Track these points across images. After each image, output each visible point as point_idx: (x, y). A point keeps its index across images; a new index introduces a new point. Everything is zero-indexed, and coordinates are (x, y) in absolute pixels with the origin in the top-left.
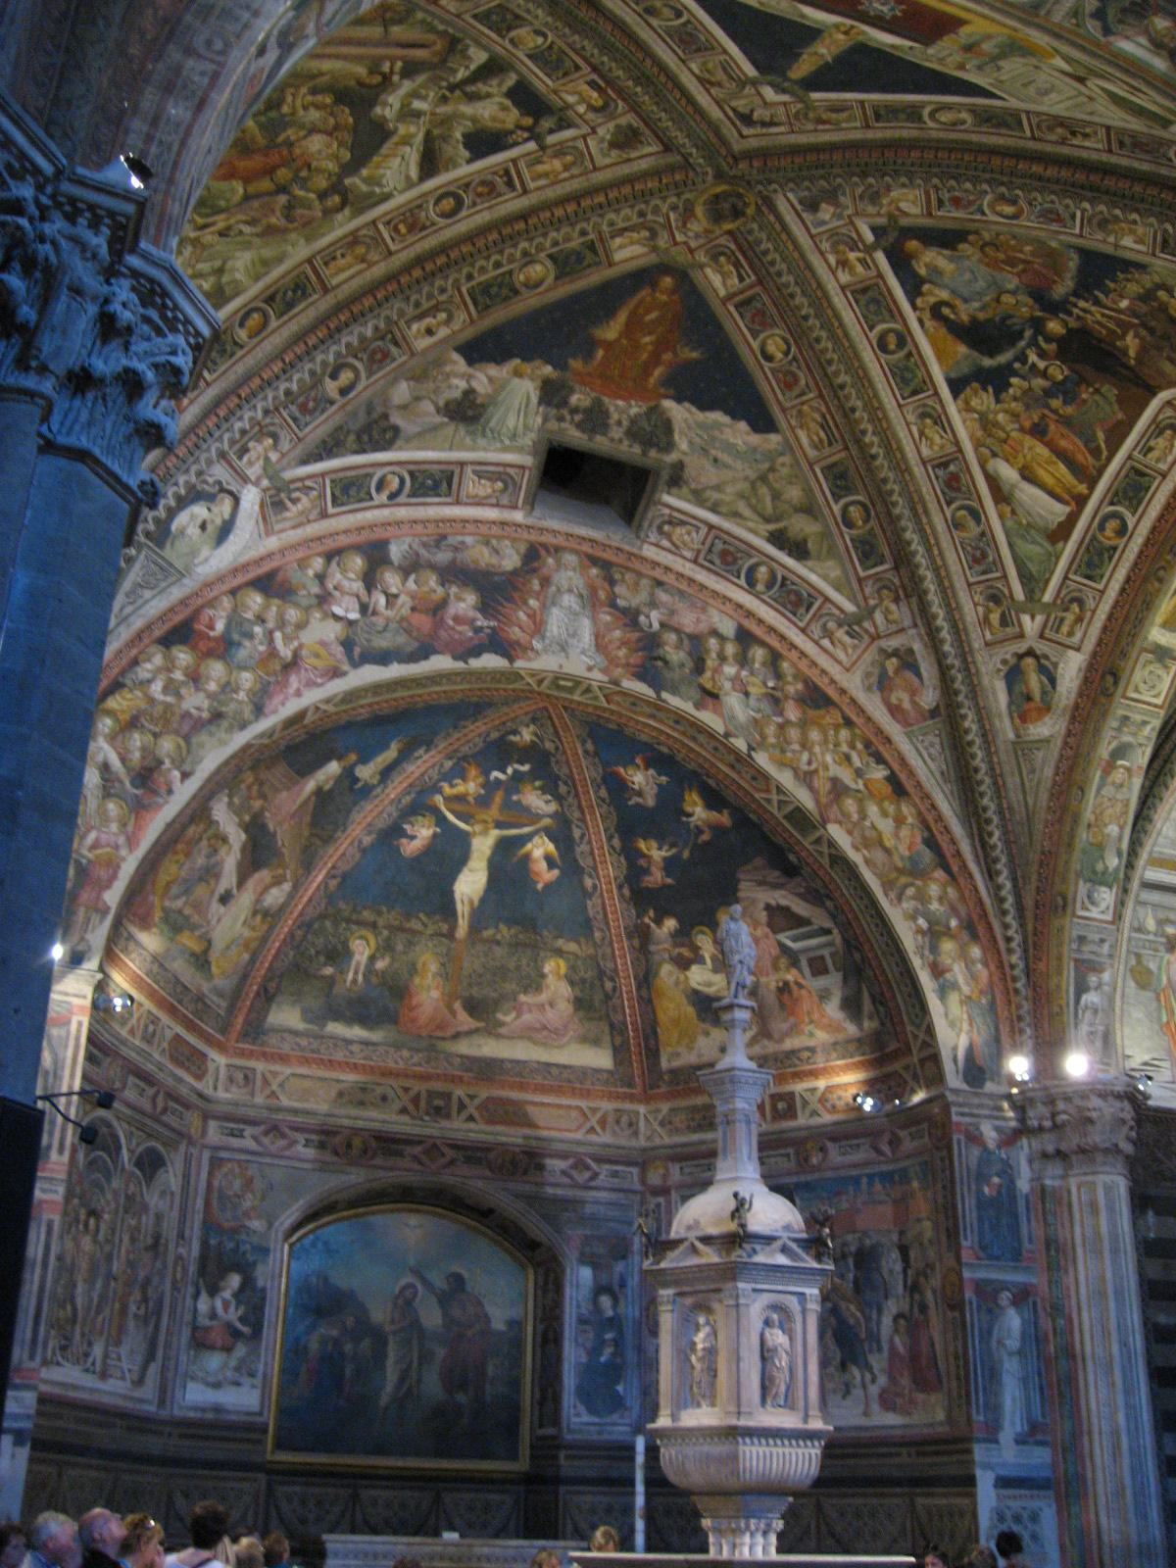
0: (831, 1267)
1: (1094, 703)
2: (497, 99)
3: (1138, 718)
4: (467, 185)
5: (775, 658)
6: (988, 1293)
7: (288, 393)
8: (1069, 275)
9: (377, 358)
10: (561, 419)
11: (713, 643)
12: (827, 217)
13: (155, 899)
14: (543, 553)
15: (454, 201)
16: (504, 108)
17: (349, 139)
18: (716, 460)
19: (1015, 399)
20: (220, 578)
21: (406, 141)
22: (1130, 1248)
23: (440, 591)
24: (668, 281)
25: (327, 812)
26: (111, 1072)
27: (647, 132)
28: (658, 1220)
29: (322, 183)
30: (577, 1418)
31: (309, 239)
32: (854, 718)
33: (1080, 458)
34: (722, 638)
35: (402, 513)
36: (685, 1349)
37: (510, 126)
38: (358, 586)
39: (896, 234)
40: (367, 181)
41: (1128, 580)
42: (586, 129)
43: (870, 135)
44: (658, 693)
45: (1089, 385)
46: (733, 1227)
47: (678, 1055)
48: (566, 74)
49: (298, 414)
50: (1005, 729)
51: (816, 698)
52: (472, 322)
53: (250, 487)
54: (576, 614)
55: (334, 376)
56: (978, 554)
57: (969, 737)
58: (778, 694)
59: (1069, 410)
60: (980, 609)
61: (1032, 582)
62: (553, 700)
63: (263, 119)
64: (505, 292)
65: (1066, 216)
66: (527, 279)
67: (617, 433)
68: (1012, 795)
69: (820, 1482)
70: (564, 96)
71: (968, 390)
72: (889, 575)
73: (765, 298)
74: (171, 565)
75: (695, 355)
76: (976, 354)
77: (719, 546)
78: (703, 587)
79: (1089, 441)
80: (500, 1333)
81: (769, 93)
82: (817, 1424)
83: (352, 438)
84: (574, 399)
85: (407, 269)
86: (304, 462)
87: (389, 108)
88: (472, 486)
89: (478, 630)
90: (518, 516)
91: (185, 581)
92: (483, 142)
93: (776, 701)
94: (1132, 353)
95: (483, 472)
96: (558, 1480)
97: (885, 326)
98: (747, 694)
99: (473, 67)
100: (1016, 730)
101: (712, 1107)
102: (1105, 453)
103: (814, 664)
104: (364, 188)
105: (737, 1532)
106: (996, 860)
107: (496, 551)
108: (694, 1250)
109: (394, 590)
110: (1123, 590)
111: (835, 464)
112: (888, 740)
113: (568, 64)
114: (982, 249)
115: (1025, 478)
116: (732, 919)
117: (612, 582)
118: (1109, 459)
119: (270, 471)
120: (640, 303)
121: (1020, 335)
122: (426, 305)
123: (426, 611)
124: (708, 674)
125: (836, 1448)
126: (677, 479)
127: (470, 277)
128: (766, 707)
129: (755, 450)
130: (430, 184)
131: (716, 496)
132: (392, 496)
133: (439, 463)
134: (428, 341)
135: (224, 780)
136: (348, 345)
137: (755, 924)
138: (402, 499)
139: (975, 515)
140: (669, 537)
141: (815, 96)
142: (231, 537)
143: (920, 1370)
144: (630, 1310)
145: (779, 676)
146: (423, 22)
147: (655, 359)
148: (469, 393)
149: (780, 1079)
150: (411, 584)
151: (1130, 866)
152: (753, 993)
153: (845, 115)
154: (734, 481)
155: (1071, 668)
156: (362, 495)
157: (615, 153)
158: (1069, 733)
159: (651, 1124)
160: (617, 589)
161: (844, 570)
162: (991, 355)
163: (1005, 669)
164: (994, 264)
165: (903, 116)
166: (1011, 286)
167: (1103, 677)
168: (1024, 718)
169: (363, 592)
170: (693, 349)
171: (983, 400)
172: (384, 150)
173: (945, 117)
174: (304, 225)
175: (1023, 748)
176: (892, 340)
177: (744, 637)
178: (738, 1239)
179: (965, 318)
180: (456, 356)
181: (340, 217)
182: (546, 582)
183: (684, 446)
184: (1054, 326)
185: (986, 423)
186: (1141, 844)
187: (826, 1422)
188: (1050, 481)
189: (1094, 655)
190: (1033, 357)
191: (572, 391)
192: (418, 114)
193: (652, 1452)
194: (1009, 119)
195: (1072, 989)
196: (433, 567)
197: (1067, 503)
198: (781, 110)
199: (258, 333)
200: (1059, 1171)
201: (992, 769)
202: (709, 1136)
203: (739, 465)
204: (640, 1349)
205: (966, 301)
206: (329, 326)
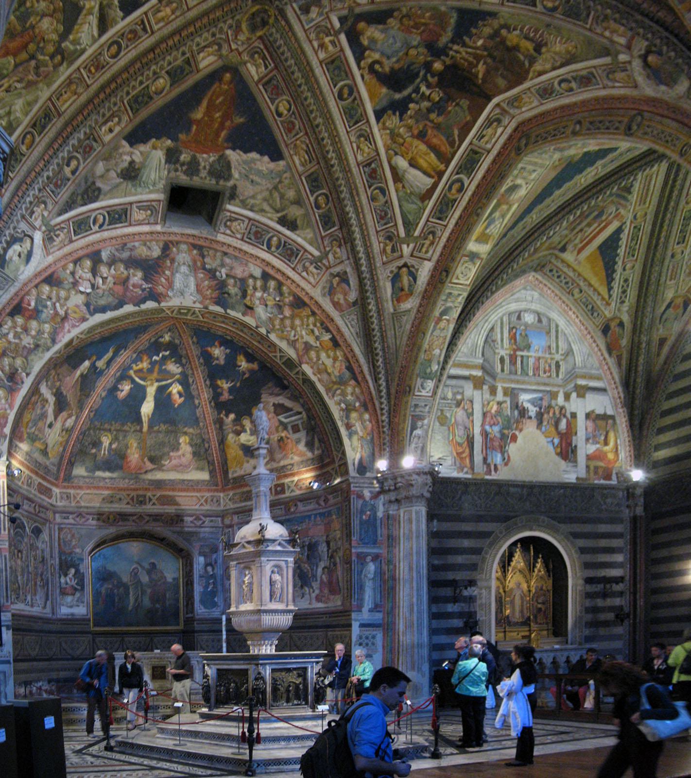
0: (298, 550)
3: (456, 293)
4: (123, 35)
6: (362, 557)
7: (48, 178)
13: (23, 429)
22: (424, 535)
25: (86, 383)
26: (17, 499)
28: (229, 537)
30: (200, 610)
31: (49, 85)
36: (240, 584)
46: (259, 537)
47: (236, 472)
54: (187, 276)
62: (179, 320)
68: (390, 340)
69: (291, 628)
76: (392, 92)
80: (170, 583)
82: (291, 607)
85: (97, 95)
94: (480, 76)
96: (194, 632)
101: (250, 491)
102: (457, 143)
105: (260, 645)
106: (379, 373)
108: (244, 547)
116: (259, 410)
120: (214, 92)
122: (108, 115)
125: (297, 616)
127: (128, 93)
129: (272, 172)
133: (120, 205)
135: (44, 375)
136: (73, 145)
137: (268, 413)
143: (333, 587)
144: (219, 571)
149: (279, 478)
150: (113, 271)
151: (443, 368)
152: (267, 443)
159: (226, 500)
164: (407, 30)
166: (415, 43)
178: (261, 541)
179: (387, 69)
184: (438, 66)
186: (450, 357)
187: (295, 605)
189: (438, 261)
190: (423, 88)
193: (229, 620)
195: (409, 429)
200: (396, 508)
201: (381, 328)
202: (249, 503)
204: (223, 585)
205: (388, 58)
206: (63, 136)
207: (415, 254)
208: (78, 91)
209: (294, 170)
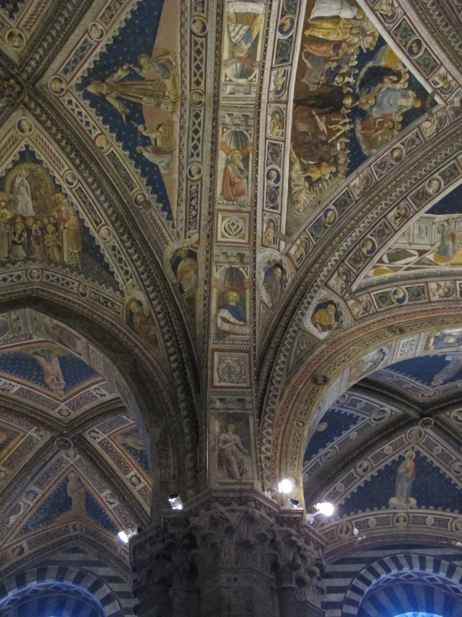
8: (361, 139)
19: (352, 54)
33: (314, 47)
45: (323, 84)
71: (375, 44)
97: (420, 54)
114: (394, 123)
115: (338, 17)
118: (300, 57)
121: (361, 86)
162: (370, 69)
165: (448, 174)
171: (367, 43)
176: (415, 49)
185: (363, 33)
188: (326, 25)
194: (419, 202)
197: (313, 19)
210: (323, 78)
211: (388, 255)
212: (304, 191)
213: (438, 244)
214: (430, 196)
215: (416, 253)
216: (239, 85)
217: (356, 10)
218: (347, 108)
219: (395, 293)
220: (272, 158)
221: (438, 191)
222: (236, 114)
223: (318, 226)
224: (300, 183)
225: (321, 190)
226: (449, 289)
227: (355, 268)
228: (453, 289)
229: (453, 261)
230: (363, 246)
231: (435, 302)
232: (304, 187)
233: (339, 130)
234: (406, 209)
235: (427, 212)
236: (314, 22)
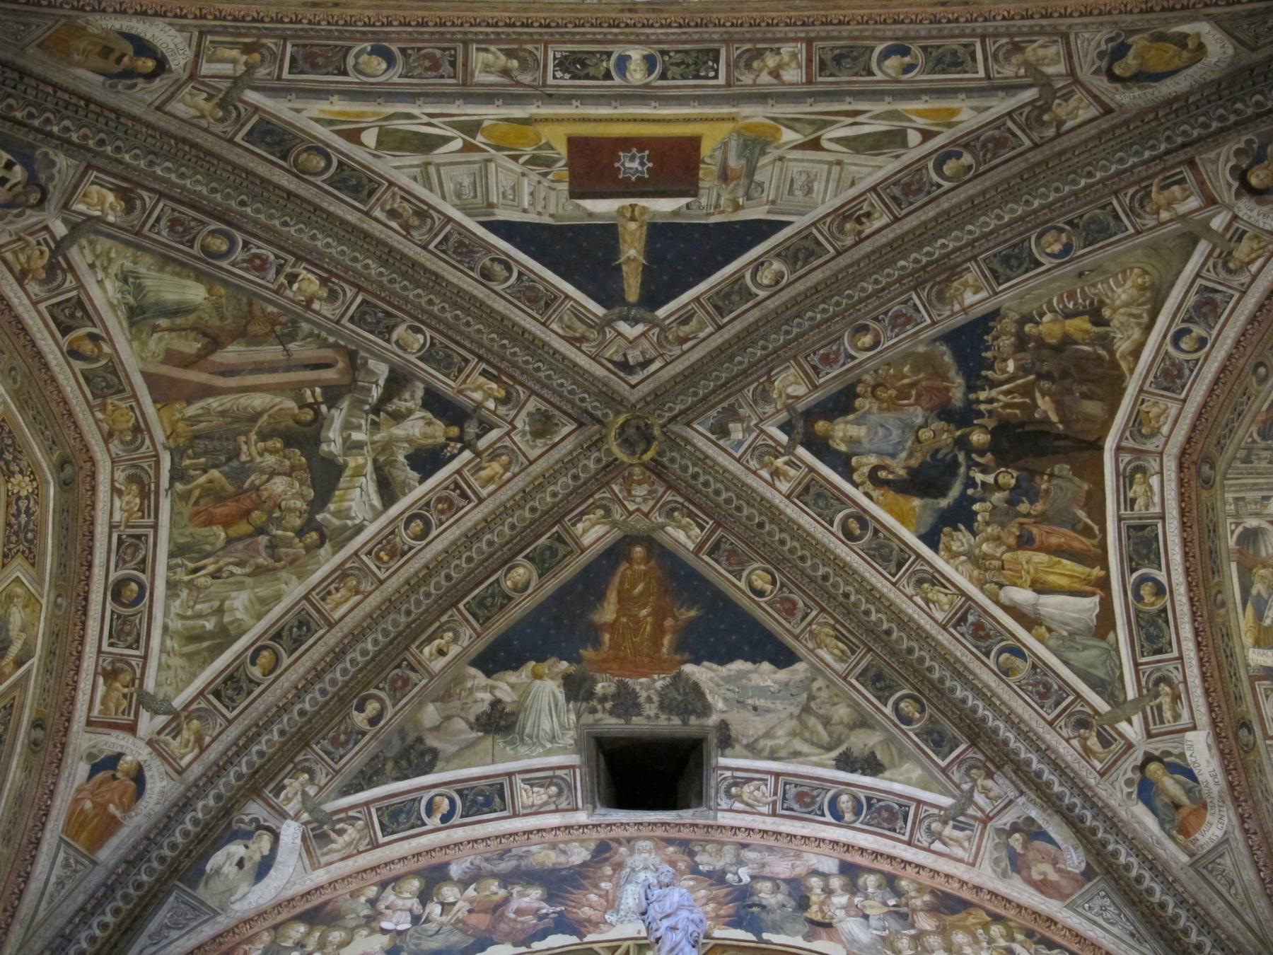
1: (1246, 769)
2: (419, 414)
5: (890, 882)
8: (952, 373)
9: (400, 687)
10: (593, 711)
11: (815, 882)
12: (740, 436)
14: (614, 845)
15: (421, 520)
16: (429, 424)
17: (306, 476)
18: (755, 709)
19: (988, 524)
20: (262, 914)
21: (359, 472)
23: (502, 893)
24: (638, 551)
27: (557, 413)
29: (298, 522)
31: (301, 577)
32: (1003, 912)
33: (1076, 545)
34: (825, 876)
35: (459, 834)
37: (442, 440)
38: (414, 903)
39: (801, 423)
40: (338, 514)
41: (1197, 632)
42: (507, 427)
43: (727, 334)
44: (758, 934)
45: (1042, 474)
48: (460, 371)
49: (330, 748)
50: (1172, 853)
51: (948, 905)
52: (479, 636)
53: (288, 821)
55: (360, 709)
56: (1041, 688)
57: (1134, 873)
58: (905, 910)
59: (1039, 507)
60: (1075, 742)
61: (1108, 687)
63: (226, 468)
64: (499, 601)
65: (911, 312)
66: (515, 584)
67: (651, 710)
70: (469, 393)
71: (943, 539)
72: (970, 754)
73: (731, 538)
74: (203, 903)
75: (693, 613)
77: (792, 791)
78: (792, 837)
79: (1074, 524)
81: (623, 327)
83: (390, 765)
84: (599, 688)
86: (345, 793)
87: (333, 442)
88: (526, 796)
89: (541, 918)
90: (582, 817)
91: (219, 919)
92: (427, 460)
93: (903, 917)
95: (536, 779)
97: (840, 515)
98: (866, 917)
99: (381, 382)
100: (1185, 849)
103: (936, 872)
104: (336, 522)
107: (564, 852)
109: (451, 900)
110: (1198, 644)
111: (865, 670)
112: (1051, 921)
113: (456, 359)
114: (874, 395)
115: (1040, 592)
117: (692, 854)
118: (1103, 530)
119: (309, 804)
121: (955, 464)
123: (485, 911)
124: (815, 908)
126: (726, 740)
128: (893, 924)
129: (787, 684)
130: (394, 510)
131: (770, 743)
132: (445, 818)
134: (442, 661)
138: (456, 820)
139: (1017, 652)
140: (738, 797)
141: (661, 313)
142: (272, 872)
145: (899, 893)
146: (311, 334)
147: (659, 630)
148: (496, 703)
153: (694, 322)
154: (781, 721)
155: (1199, 750)
156: (413, 820)
157: (539, 442)
158: (1242, 819)
160: (698, 859)
161: (924, 767)
162: (943, 494)
163: (1135, 789)
165: (735, 298)
167: (1236, 737)
168: (1185, 830)
169: (417, 908)
170: (689, 609)
171: (961, 540)
172: (343, 482)
173: (766, 277)
174: (292, 563)
175: (1204, 864)
176: (854, 525)
177: (850, 871)
180: (473, 671)
181: (322, 552)
182: (618, 866)
183: (720, 705)
185: (977, 560)
188: (1064, 582)
189: (1214, 723)
191: (595, 682)
192: (359, 445)
194: (807, 243)
196: (494, 875)
197: (1093, 594)
198: (646, 344)
199: (271, 672)
203: (779, 706)
207: (1154, 729)
208: (362, 588)
209: (828, 672)
210: (1044, 486)
211: (904, 144)
212: (1118, 303)
213: (764, 161)
214: (778, 255)
215: (825, 144)
216: (1257, 515)
217: (1003, 599)
218: (981, 426)
219: (908, 68)
220: (1180, 371)
221: (758, 265)
222: (1264, 464)
223: (1097, 232)
224: (1124, 319)
225: (1072, 296)
226: (748, 66)
227: (1009, 130)
228: (737, 67)
229: (729, 126)
230: (970, 167)
231: (795, 40)
232: (1114, 311)
233: (1006, 393)
234: (841, 231)
235: (789, 223)
236: (1088, 588)
